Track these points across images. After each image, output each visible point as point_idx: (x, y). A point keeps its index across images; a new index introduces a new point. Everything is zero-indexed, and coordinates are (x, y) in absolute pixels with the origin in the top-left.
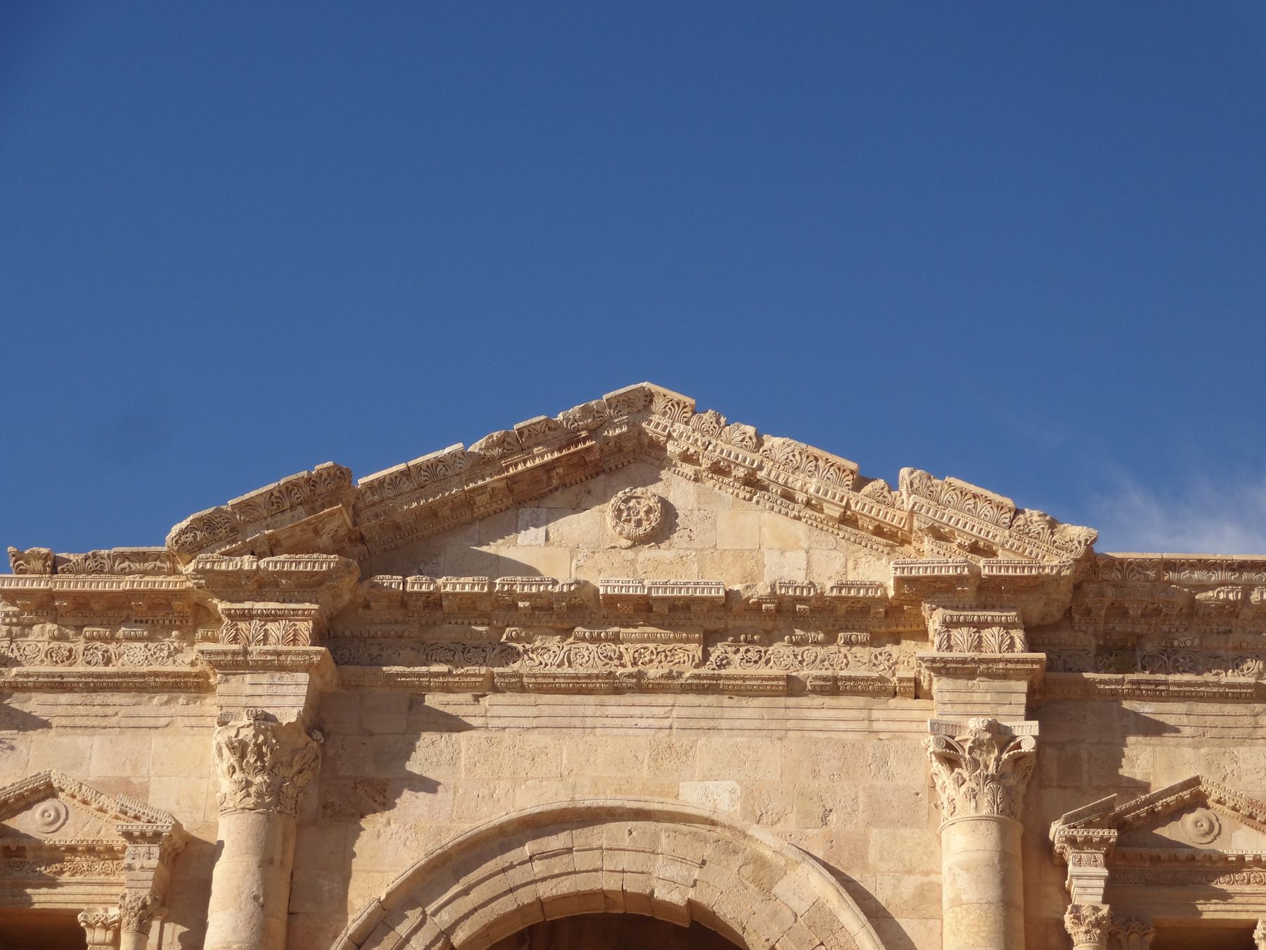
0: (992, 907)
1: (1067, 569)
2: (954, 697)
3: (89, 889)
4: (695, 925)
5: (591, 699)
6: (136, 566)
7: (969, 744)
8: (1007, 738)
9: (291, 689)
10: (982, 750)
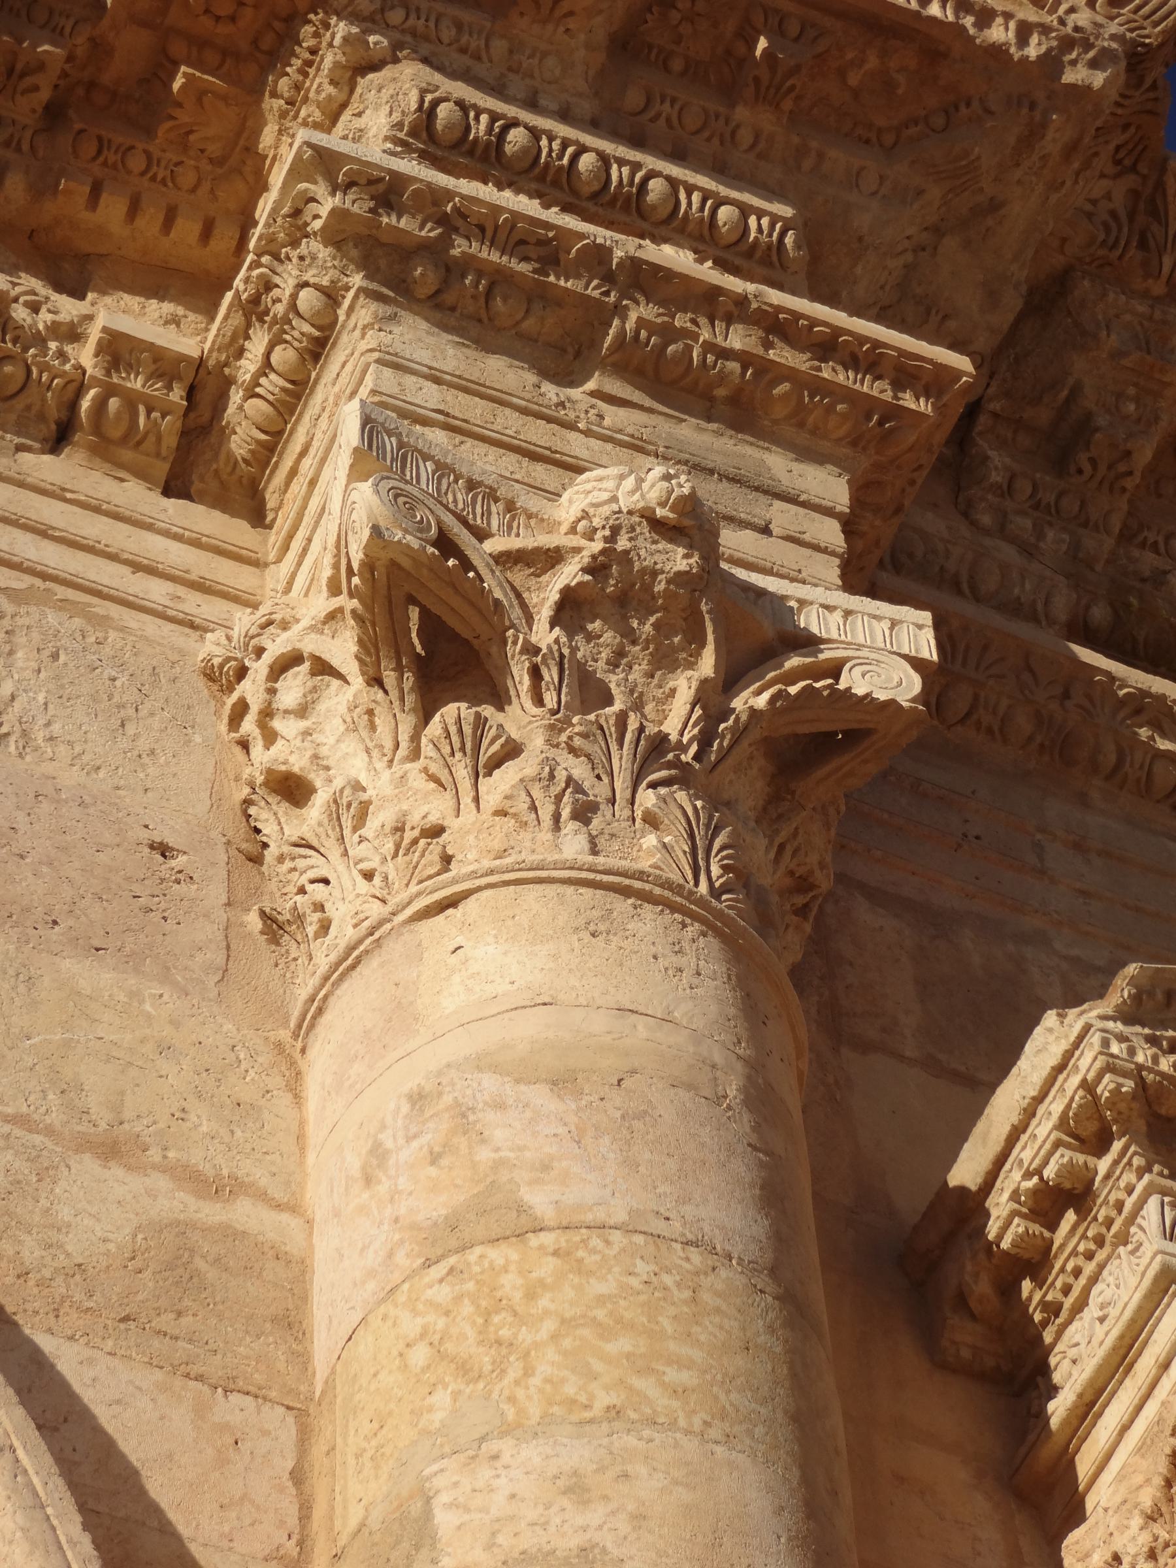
0: (723, 1273)
1: (1094, 64)
7: (569, 574)
8: (769, 631)
10: (631, 636)
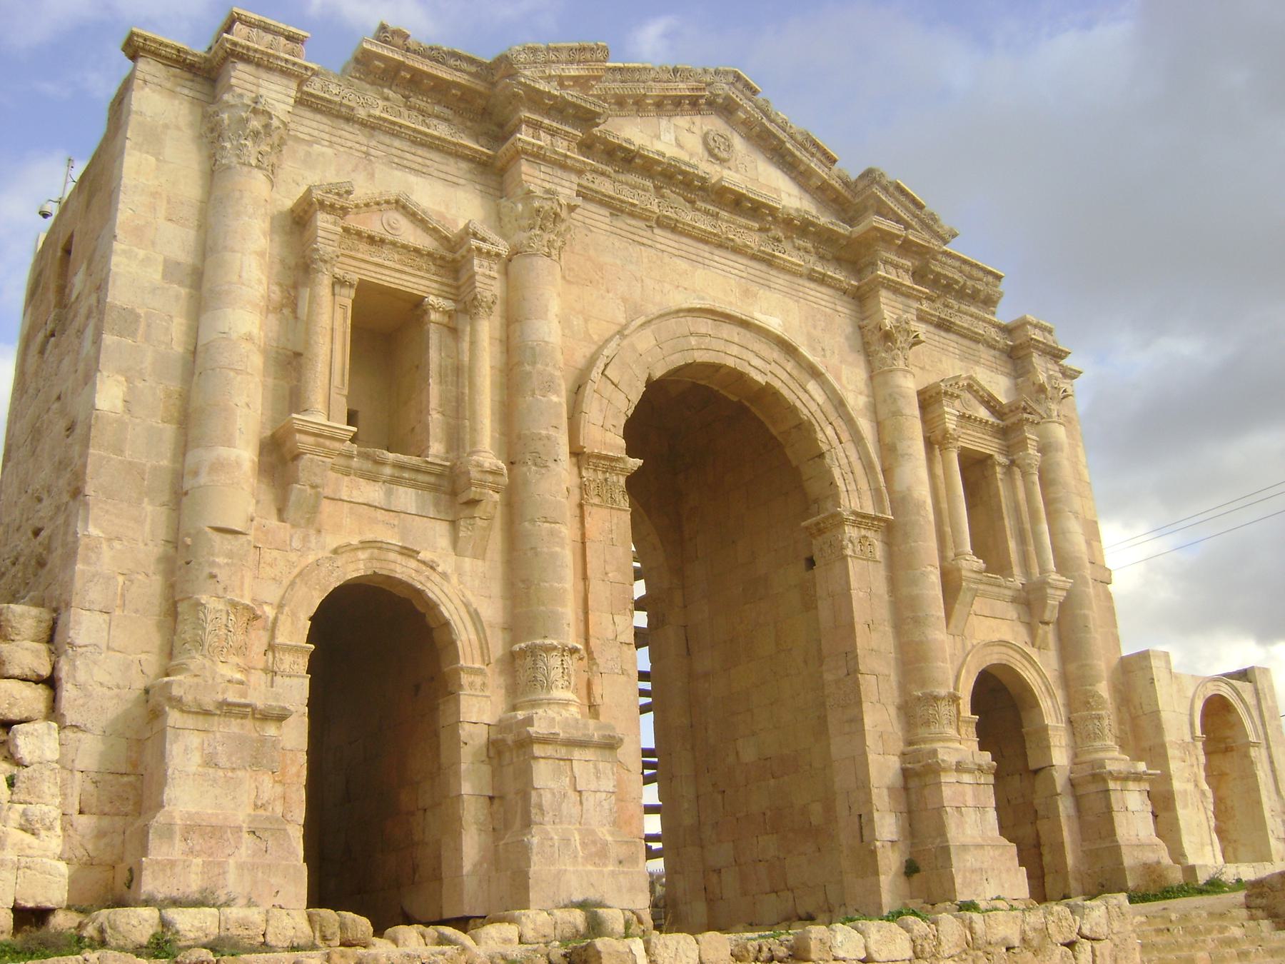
2: (887, 301)
3: (427, 283)
5: (706, 248)
6: (465, 66)
9: (567, 184)
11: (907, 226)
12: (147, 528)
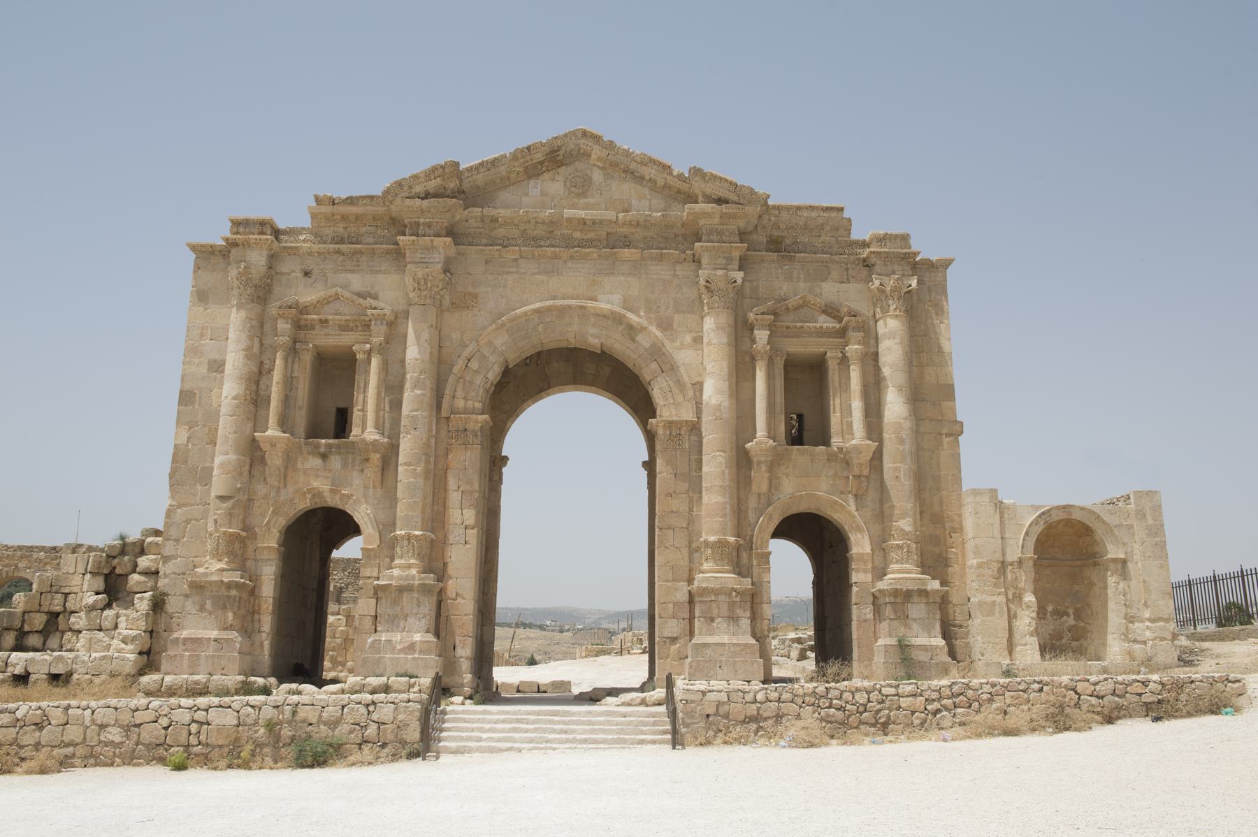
4: (603, 352)
11: (720, 201)
12: (198, 497)
